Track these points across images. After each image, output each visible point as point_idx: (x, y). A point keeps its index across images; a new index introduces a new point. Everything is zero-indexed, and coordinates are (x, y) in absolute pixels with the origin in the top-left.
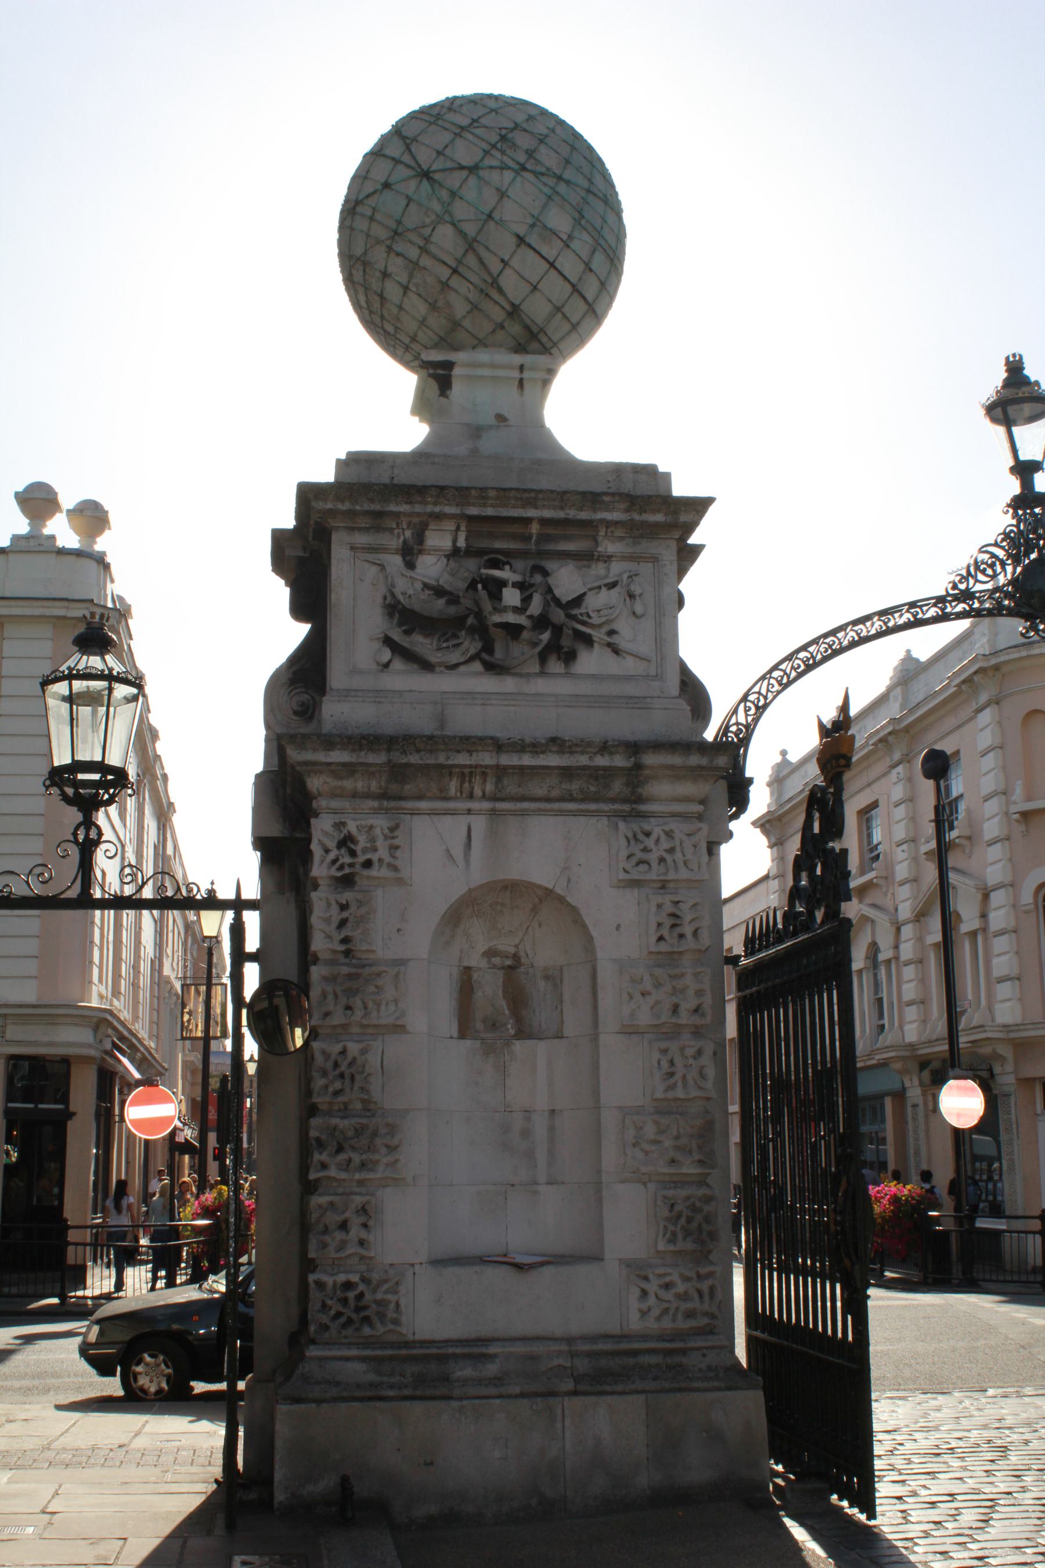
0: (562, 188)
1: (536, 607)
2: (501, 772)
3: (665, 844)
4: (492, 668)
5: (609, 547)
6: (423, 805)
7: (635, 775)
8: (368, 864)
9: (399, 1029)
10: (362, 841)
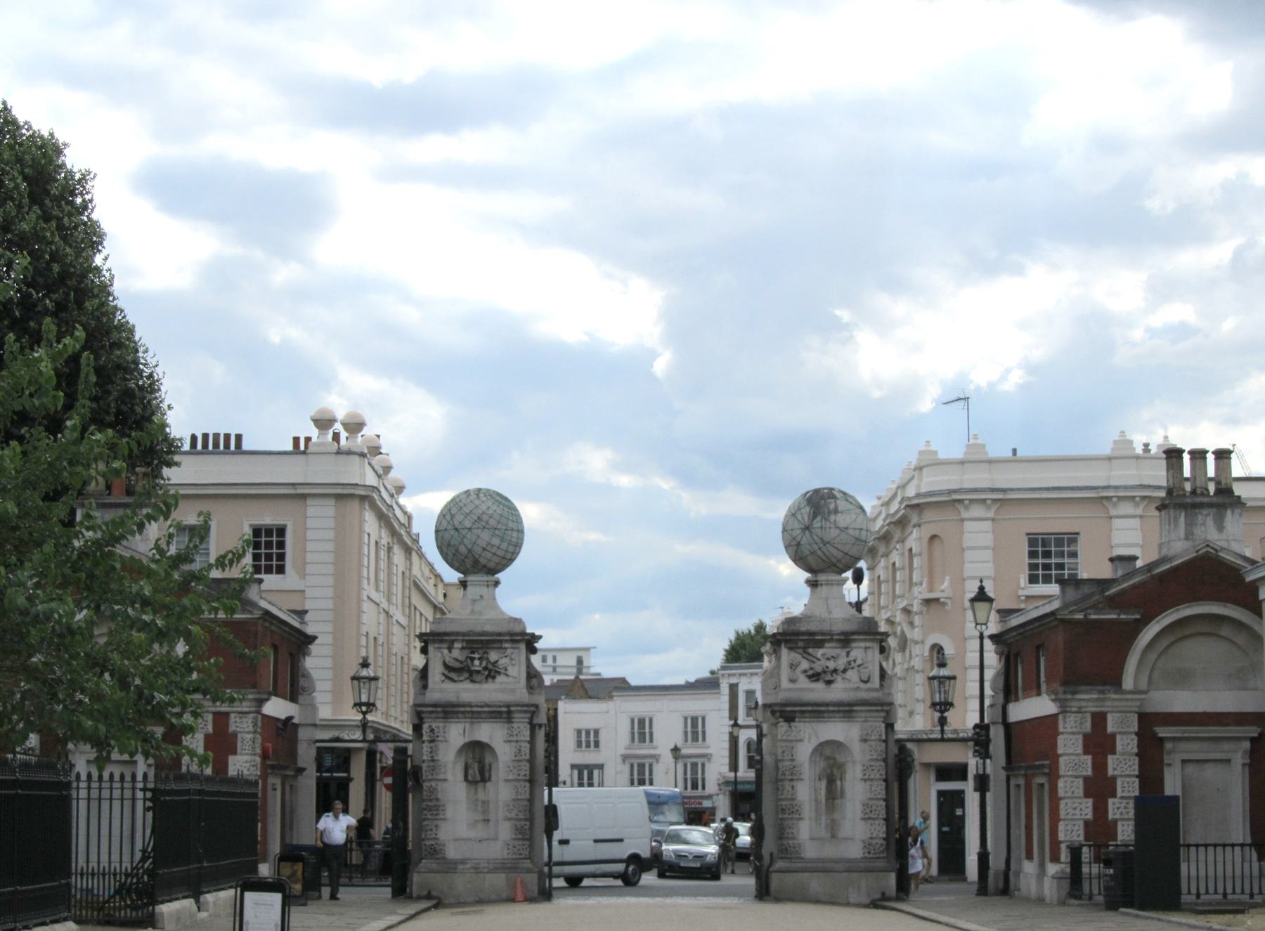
0: (497, 532)
1: (484, 664)
2: (473, 712)
3: (518, 730)
4: (473, 681)
5: (507, 645)
6: (453, 720)
7: (509, 712)
8: (438, 736)
9: (445, 780)
10: (436, 730)
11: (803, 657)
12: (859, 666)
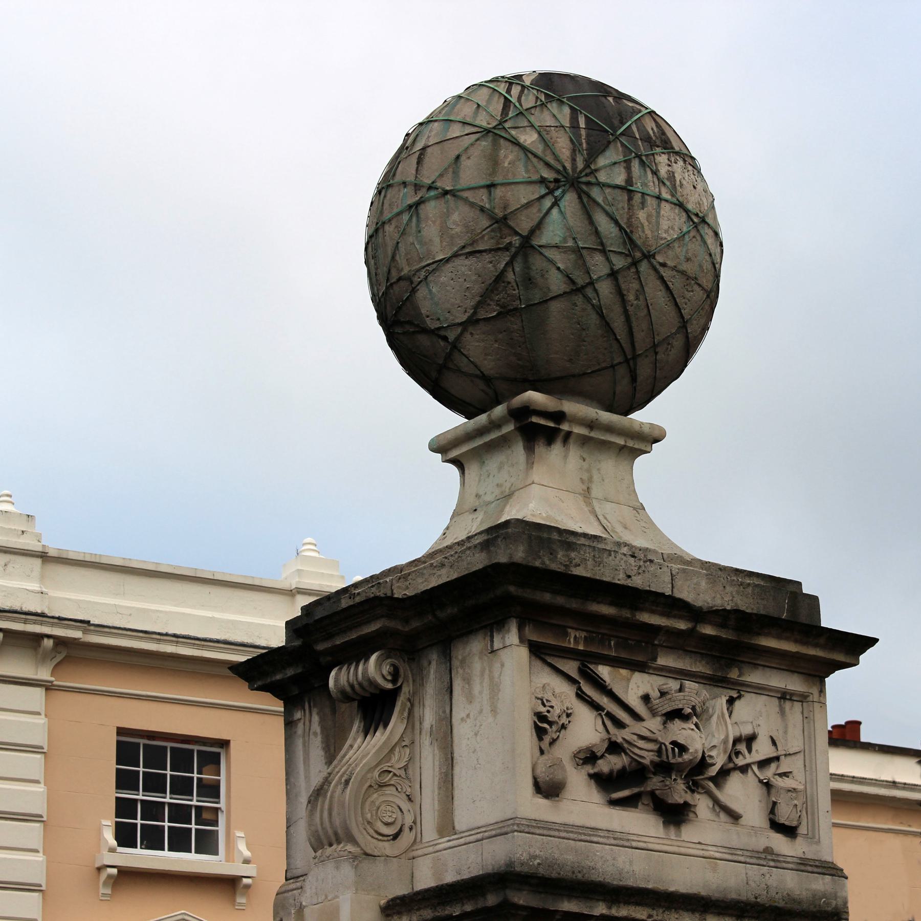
11: (581, 696)
12: (764, 764)
